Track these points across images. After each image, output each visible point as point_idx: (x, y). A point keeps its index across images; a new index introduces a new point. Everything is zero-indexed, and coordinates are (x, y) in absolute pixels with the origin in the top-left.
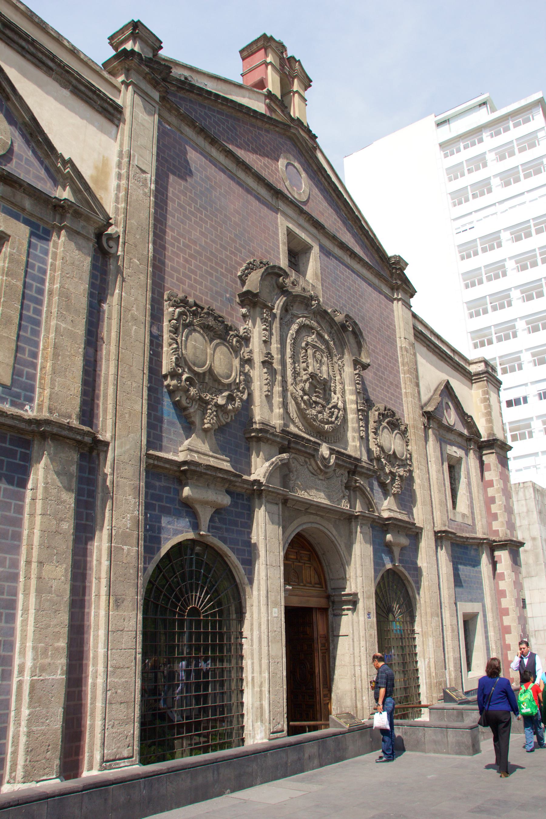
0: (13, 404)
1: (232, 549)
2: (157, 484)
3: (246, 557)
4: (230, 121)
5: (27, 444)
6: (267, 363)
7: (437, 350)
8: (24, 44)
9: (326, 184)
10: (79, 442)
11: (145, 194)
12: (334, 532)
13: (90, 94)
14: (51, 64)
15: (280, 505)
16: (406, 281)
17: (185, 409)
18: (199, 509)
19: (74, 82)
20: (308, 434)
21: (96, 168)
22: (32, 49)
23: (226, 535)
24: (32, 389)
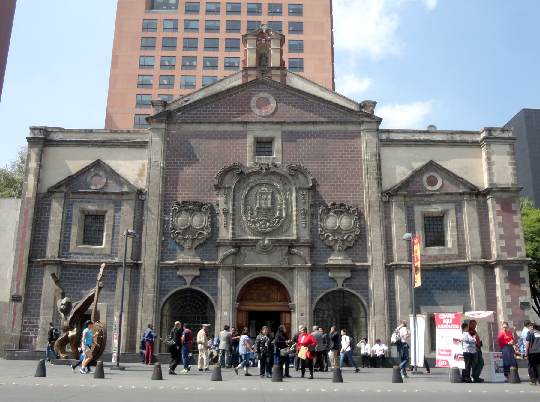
0: (112, 259)
1: (206, 291)
2: (167, 272)
3: (214, 292)
4: (213, 104)
5: (116, 269)
6: (226, 212)
7: (420, 143)
8: (109, 144)
9: (292, 92)
10: (130, 266)
11: (158, 170)
12: (280, 276)
13: (135, 144)
14: (118, 144)
15: (232, 271)
16: (371, 116)
17: (179, 243)
18: (185, 277)
19: (128, 144)
20: (256, 235)
21: (140, 170)
22: (112, 144)
23: (202, 285)
24: (117, 253)
